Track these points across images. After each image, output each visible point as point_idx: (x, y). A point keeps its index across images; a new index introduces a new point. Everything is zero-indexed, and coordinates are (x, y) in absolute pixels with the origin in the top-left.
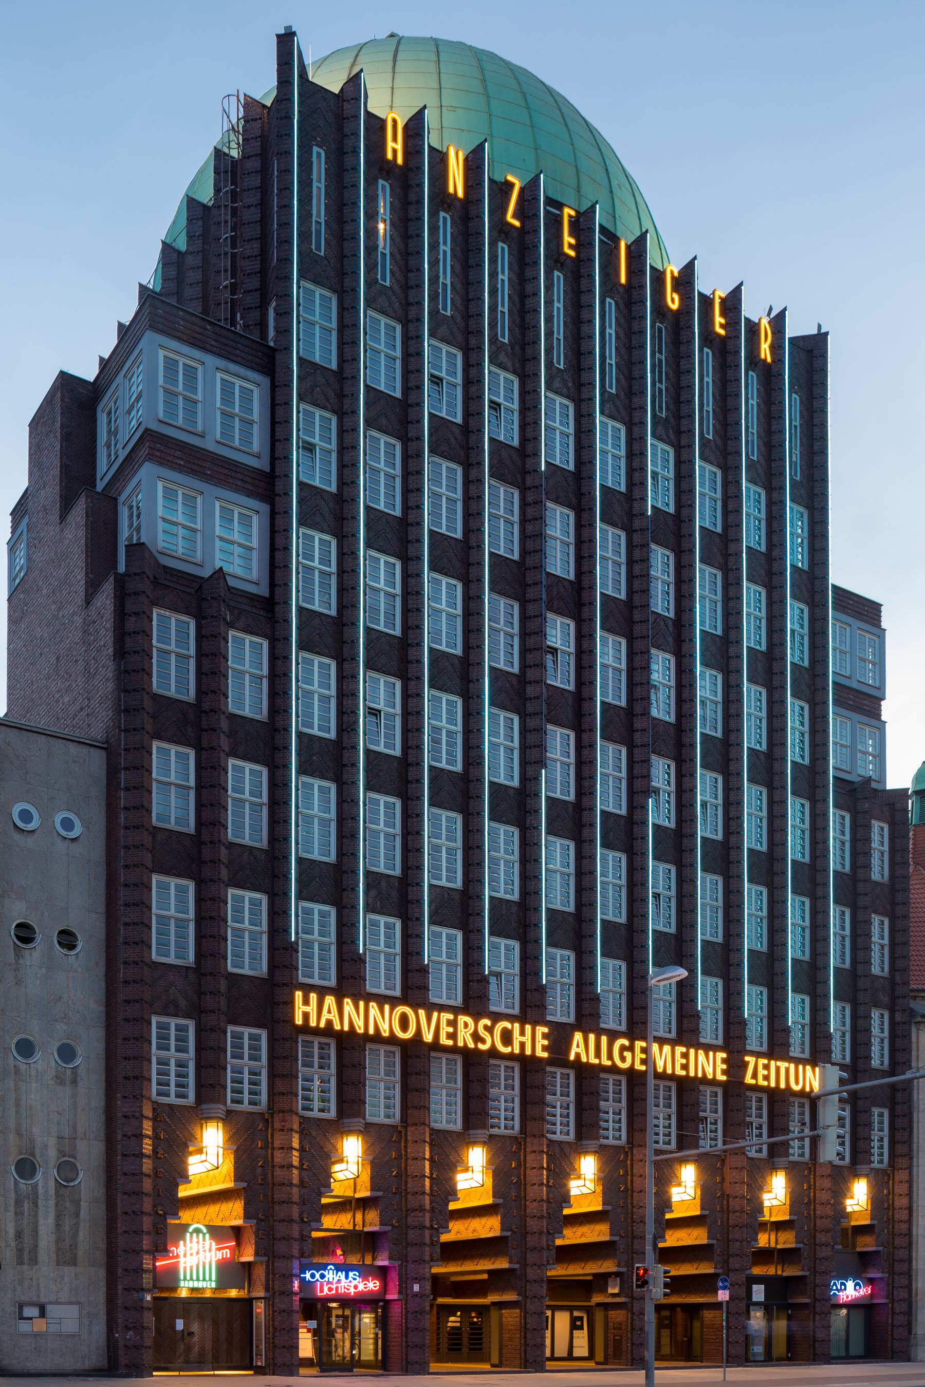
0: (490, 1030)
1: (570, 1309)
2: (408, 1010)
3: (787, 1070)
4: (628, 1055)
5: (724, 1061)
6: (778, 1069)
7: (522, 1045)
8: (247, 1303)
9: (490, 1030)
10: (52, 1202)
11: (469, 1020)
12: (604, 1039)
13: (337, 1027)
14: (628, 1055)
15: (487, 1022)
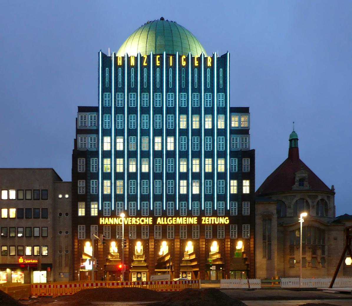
0: (139, 220)
3: (214, 219)
4: (171, 221)
6: (211, 220)
7: (146, 222)
9: (139, 220)
10: (64, 256)
12: (165, 218)
14: (171, 221)
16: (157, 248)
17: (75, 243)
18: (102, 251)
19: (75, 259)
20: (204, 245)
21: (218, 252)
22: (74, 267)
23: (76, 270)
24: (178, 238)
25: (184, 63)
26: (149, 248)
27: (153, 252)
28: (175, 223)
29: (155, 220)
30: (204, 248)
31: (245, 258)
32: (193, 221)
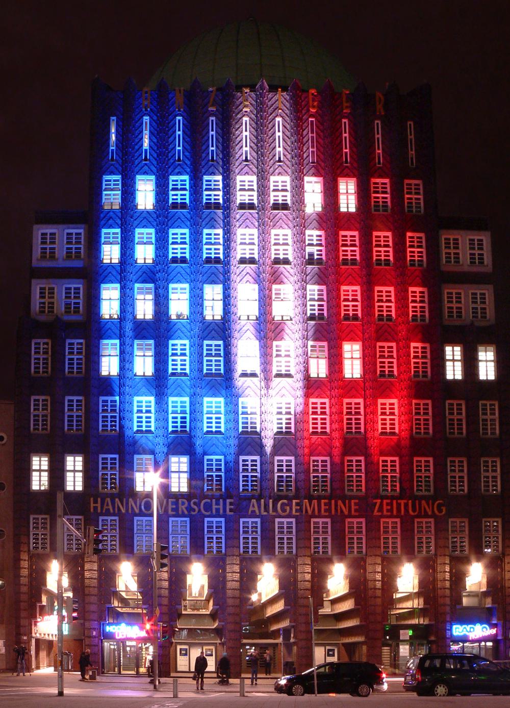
0: (198, 504)
1: (324, 645)
5: (355, 504)
6: (399, 505)
7: (218, 510)
9: (198, 504)
16: (249, 580)
17: (22, 562)
18: (94, 587)
19: (22, 604)
20: (379, 572)
21: (415, 593)
22: (18, 626)
23: (25, 635)
24: (309, 554)
26: (224, 581)
27: (238, 591)
30: (380, 583)
31: (488, 608)
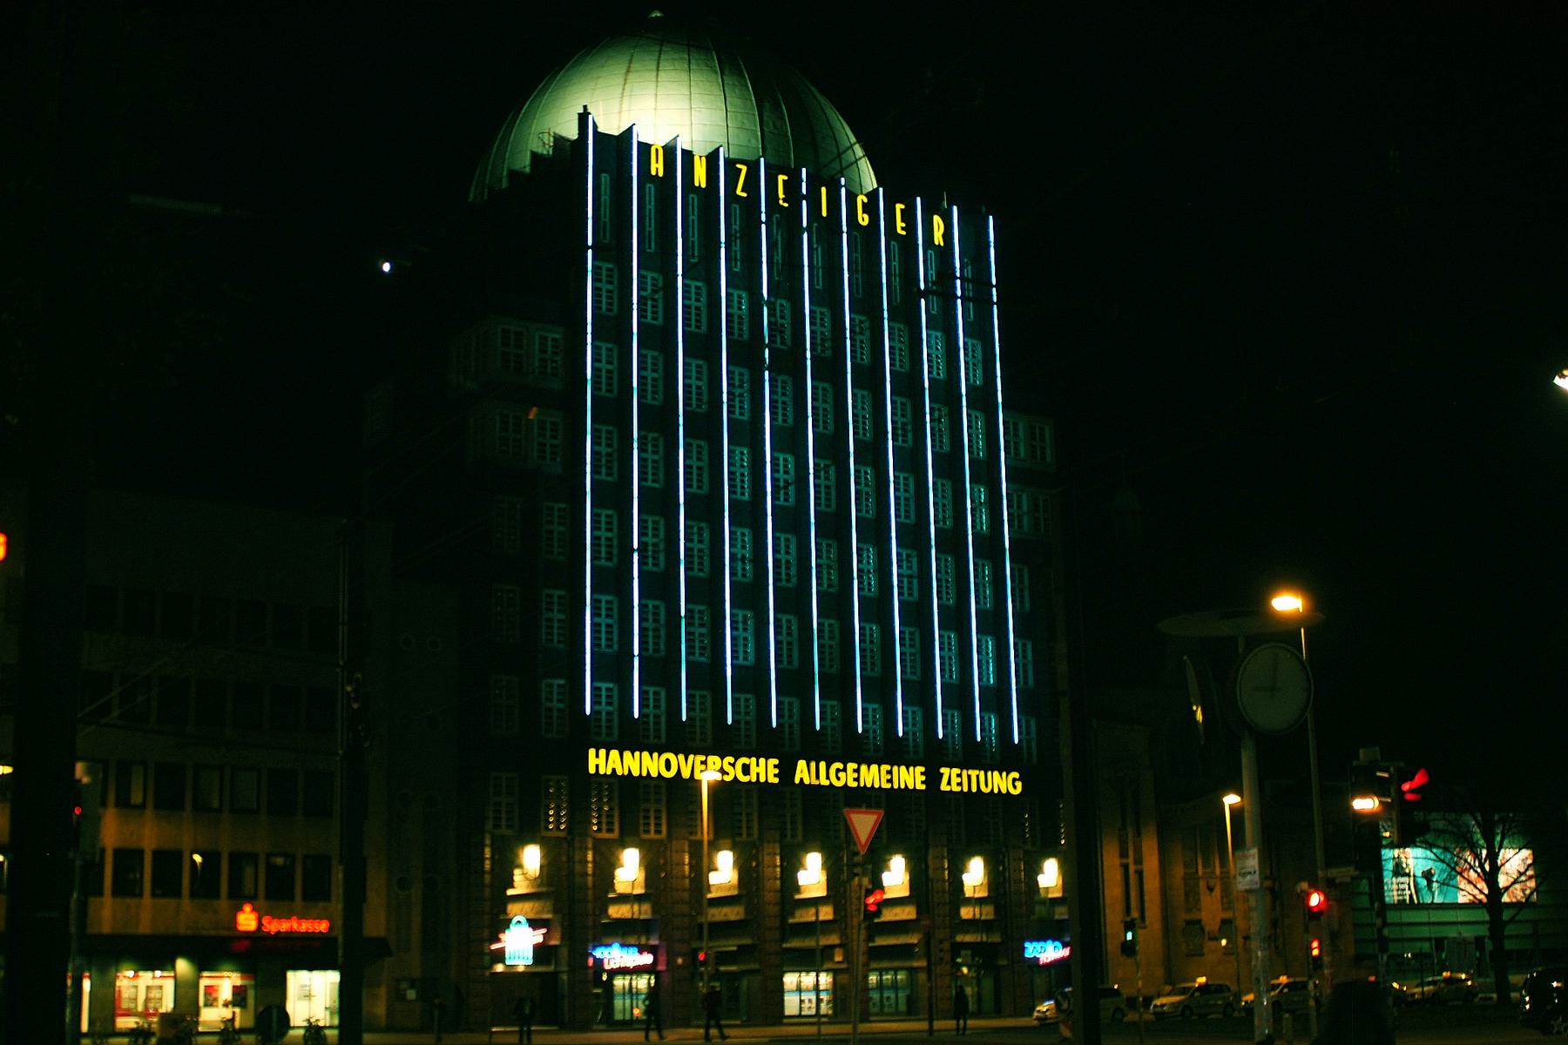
0: (733, 765)
2: (671, 756)
8: (555, 974)
9: (733, 765)
11: (716, 759)
12: (823, 765)
13: (619, 773)
14: (842, 775)
15: (731, 759)
25: (863, 219)
28: (855, 784)
29: (787, 771)
32: (911, 778)
